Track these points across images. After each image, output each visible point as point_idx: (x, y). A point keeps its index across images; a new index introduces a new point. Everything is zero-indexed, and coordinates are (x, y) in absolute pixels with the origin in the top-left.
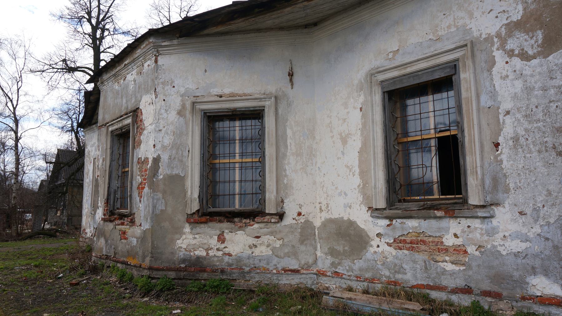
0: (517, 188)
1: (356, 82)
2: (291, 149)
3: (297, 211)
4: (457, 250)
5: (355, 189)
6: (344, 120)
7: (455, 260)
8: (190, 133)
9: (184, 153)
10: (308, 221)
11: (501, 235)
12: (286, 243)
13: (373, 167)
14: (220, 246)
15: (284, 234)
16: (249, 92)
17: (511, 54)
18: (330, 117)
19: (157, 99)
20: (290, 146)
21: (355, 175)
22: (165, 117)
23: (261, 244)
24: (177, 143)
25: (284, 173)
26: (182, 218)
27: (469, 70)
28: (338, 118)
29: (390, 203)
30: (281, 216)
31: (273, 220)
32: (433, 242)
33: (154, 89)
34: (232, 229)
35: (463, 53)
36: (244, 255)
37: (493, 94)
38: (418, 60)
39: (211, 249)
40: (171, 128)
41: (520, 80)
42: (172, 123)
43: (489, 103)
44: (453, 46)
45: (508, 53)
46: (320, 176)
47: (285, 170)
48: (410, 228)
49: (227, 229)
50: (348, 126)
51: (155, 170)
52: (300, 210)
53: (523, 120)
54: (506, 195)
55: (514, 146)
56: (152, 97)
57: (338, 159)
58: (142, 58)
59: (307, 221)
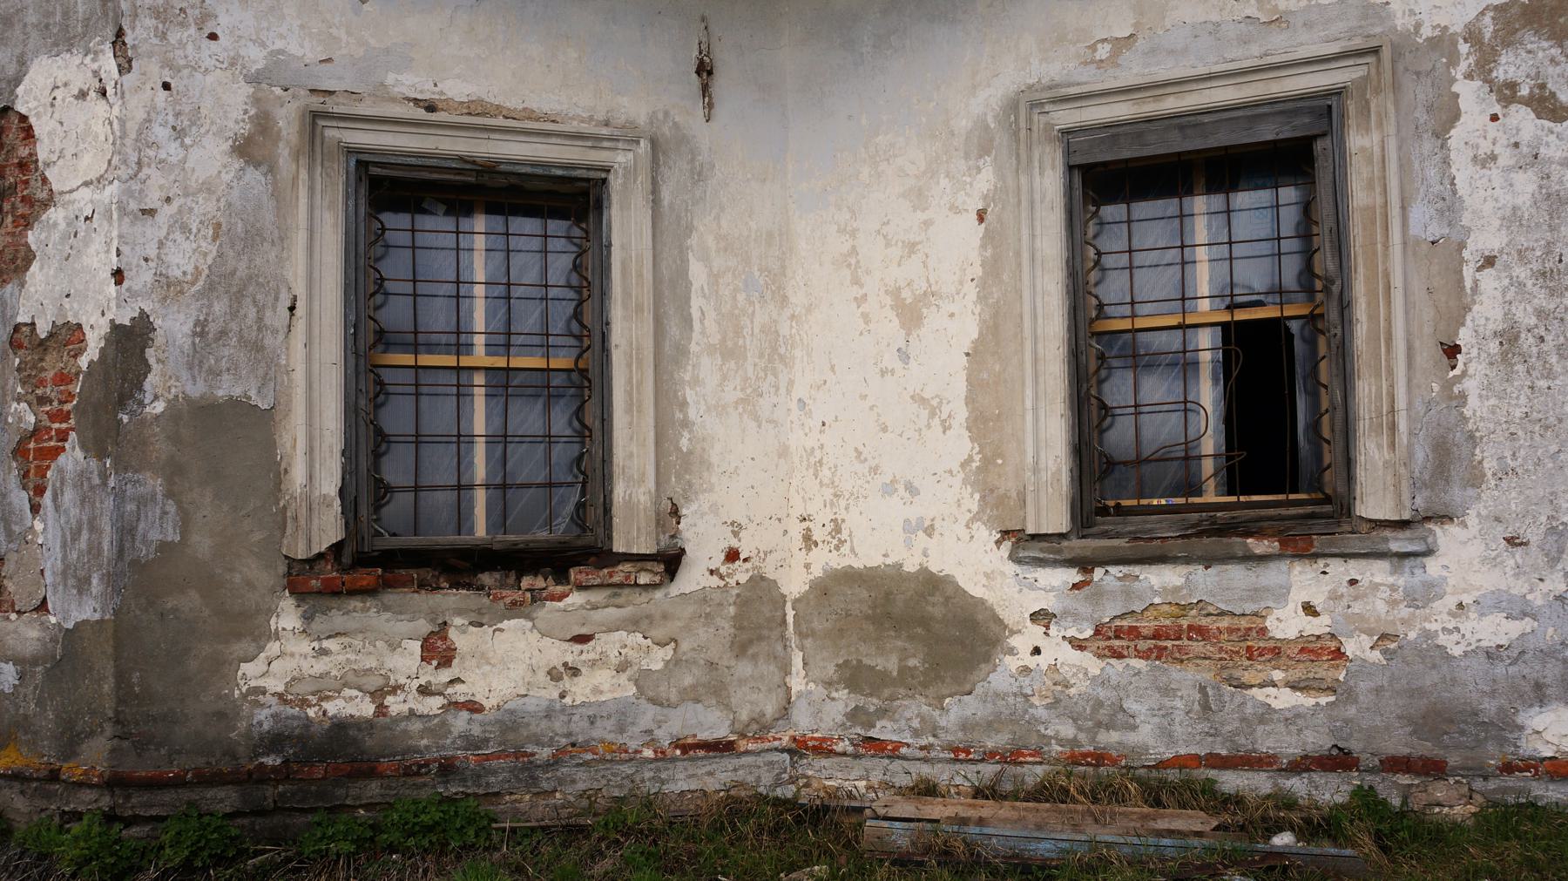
0: (1505, 472)
2: (703, 333)
3: (724, 545)
4: (1311, 651)
5: (951, 472)
7: (1303, 677)
8: (301, 238)
9: (268, 313)
10: (763, 578)
11: (1450, 601)
12: (685, 653)
13: (1029, 404)
14: (432, 679)
15: (679, 624)
16: (546, 108)
17: (1507, 93)
18: (853, 233)
19: (128, 79)
20: (702, 321)
21: (950, 427)
22: (173, 160)
23: (593, 664)
24: (233, 273)
25: (679, 415)
26: (260, 575)
27: (1380, 125)
28: (885, 237)
30: (671, 562)
31: (644, 579)
32: (1230, 631)
33: (110, 33)
34: (479, 612)
35: (1361, 73)
36: (531, 705)
38: (1210, 77)
39: (395, 690)
41: (1530, 173)
42: (207, 188)
44: (1334, 48)
45: (1500, 91)
46: (807, 430)
47: (683, 405)
48: (1156, 593)
49: (459, 612)
50: (925, 266)
51: (124, 380)
52: (734, 543)
53: (1534, 285)
54: (1471, 492)
55: (1504, 355)
56: (95, 66)
57: (883, 373)
59: (758, 581)
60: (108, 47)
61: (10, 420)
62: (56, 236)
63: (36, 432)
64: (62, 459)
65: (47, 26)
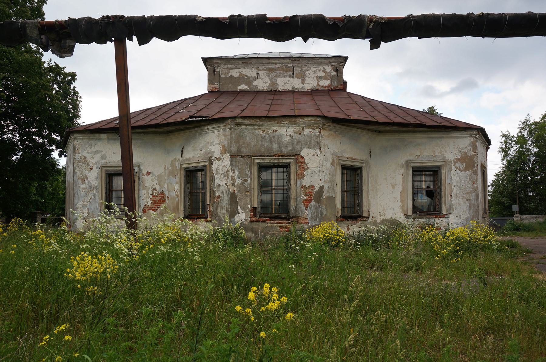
1: (400, 163)
6: (393, 178)
18: (386, 175)
29: (414, 212)
37: (451, 180)
40: (328, 171)
42: (328, 169)
43: (450, 182)
49: (350, 224)
59: (375, 220)
62: (309, 173)
63: (306, 200)
64: (311, 203)
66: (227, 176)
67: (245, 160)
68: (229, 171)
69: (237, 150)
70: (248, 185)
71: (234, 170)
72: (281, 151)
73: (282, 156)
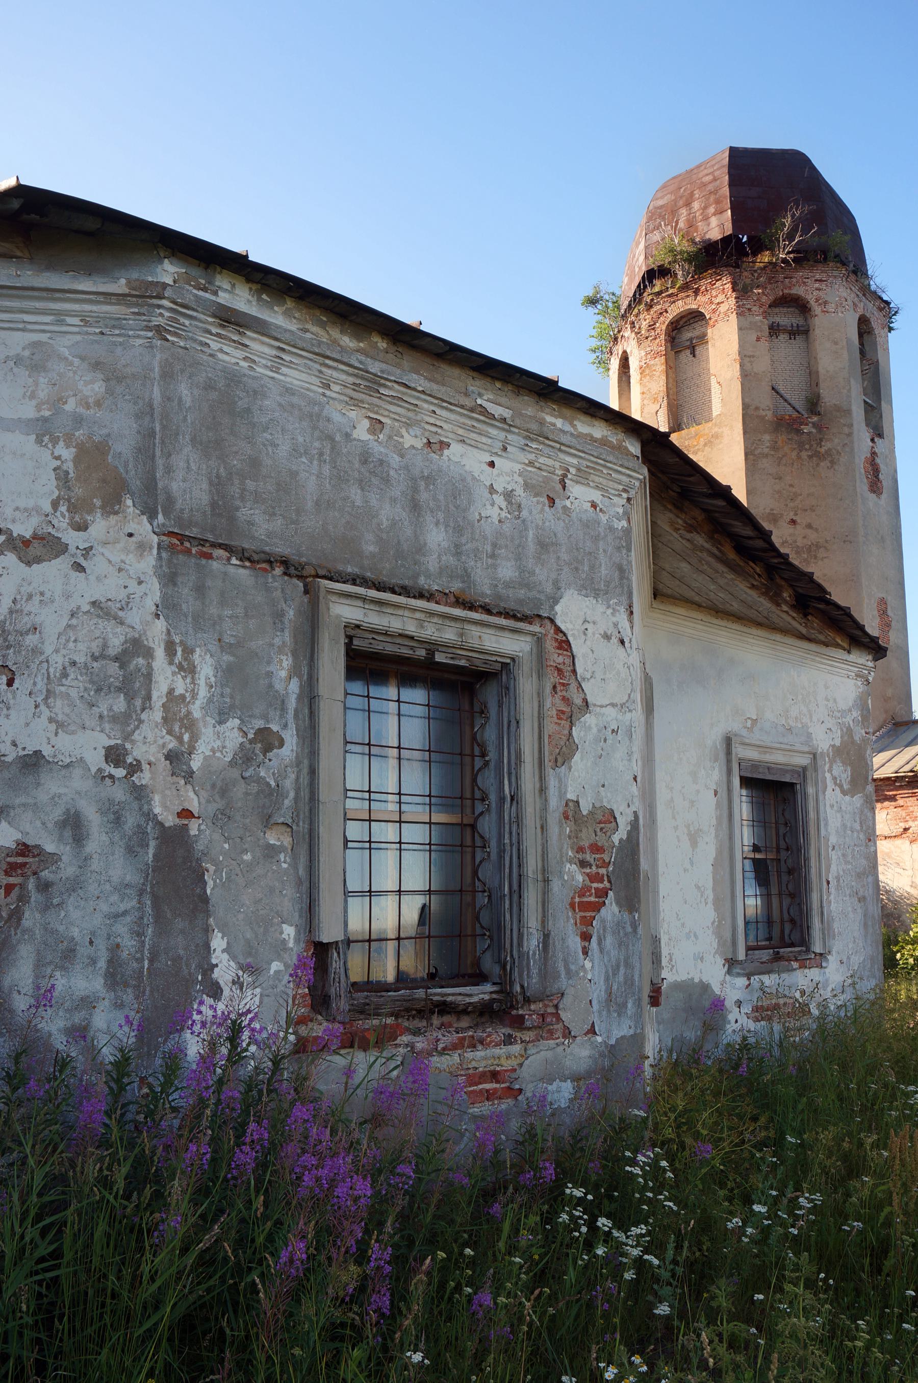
33: (624, 599)
56: (614, 619)
58: (574, 461)
60: (622, 610)
61: (566, 878)
63: (583, 891)
65: (577, 569)
66: (126, 688)
67: (268, 589)
68: (149, 653)
69: (214, 505)
70: (280, 776)
71: (188, 651)
72: (466, 576)
73: (471, 607)
